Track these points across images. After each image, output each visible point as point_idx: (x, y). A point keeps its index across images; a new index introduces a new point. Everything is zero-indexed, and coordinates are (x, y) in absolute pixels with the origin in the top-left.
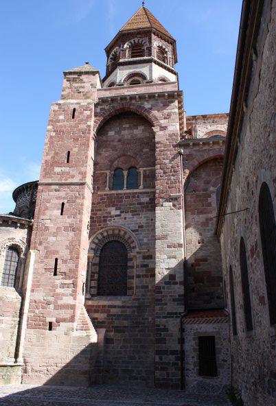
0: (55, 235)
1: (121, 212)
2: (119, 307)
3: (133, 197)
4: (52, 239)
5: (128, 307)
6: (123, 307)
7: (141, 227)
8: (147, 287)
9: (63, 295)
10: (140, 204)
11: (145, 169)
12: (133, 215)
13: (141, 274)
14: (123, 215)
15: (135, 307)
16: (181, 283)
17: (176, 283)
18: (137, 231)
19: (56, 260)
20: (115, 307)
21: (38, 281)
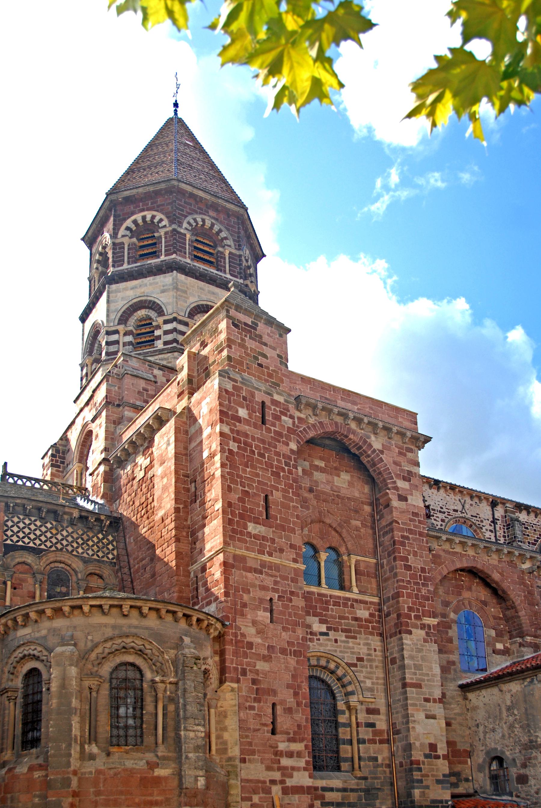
0: (267, 659)
1: (329, 628)
2: (338, 790)
3: (345, 605)
4: (261, 666)
5: (352, 790)
6: (344, 790)
7: (360, 659)
8: (376, 759)
9: (293, 768)
10: (356, 619)
11: (359, 558)
12: (347, 637)
13: (366, 737)
14: (331, 633)
15: (361, 790)
16: (445, 757)
17: (437, 757)
18: (355, 665)
19: (274, 705)
20: (331, 790)
21: (250, 744)
